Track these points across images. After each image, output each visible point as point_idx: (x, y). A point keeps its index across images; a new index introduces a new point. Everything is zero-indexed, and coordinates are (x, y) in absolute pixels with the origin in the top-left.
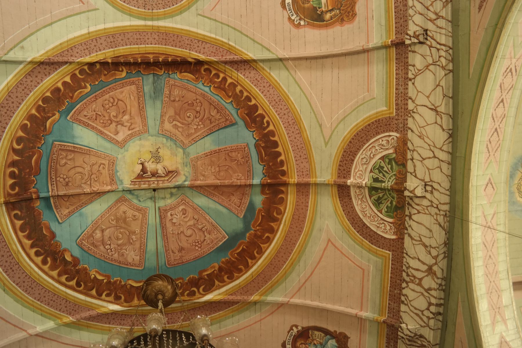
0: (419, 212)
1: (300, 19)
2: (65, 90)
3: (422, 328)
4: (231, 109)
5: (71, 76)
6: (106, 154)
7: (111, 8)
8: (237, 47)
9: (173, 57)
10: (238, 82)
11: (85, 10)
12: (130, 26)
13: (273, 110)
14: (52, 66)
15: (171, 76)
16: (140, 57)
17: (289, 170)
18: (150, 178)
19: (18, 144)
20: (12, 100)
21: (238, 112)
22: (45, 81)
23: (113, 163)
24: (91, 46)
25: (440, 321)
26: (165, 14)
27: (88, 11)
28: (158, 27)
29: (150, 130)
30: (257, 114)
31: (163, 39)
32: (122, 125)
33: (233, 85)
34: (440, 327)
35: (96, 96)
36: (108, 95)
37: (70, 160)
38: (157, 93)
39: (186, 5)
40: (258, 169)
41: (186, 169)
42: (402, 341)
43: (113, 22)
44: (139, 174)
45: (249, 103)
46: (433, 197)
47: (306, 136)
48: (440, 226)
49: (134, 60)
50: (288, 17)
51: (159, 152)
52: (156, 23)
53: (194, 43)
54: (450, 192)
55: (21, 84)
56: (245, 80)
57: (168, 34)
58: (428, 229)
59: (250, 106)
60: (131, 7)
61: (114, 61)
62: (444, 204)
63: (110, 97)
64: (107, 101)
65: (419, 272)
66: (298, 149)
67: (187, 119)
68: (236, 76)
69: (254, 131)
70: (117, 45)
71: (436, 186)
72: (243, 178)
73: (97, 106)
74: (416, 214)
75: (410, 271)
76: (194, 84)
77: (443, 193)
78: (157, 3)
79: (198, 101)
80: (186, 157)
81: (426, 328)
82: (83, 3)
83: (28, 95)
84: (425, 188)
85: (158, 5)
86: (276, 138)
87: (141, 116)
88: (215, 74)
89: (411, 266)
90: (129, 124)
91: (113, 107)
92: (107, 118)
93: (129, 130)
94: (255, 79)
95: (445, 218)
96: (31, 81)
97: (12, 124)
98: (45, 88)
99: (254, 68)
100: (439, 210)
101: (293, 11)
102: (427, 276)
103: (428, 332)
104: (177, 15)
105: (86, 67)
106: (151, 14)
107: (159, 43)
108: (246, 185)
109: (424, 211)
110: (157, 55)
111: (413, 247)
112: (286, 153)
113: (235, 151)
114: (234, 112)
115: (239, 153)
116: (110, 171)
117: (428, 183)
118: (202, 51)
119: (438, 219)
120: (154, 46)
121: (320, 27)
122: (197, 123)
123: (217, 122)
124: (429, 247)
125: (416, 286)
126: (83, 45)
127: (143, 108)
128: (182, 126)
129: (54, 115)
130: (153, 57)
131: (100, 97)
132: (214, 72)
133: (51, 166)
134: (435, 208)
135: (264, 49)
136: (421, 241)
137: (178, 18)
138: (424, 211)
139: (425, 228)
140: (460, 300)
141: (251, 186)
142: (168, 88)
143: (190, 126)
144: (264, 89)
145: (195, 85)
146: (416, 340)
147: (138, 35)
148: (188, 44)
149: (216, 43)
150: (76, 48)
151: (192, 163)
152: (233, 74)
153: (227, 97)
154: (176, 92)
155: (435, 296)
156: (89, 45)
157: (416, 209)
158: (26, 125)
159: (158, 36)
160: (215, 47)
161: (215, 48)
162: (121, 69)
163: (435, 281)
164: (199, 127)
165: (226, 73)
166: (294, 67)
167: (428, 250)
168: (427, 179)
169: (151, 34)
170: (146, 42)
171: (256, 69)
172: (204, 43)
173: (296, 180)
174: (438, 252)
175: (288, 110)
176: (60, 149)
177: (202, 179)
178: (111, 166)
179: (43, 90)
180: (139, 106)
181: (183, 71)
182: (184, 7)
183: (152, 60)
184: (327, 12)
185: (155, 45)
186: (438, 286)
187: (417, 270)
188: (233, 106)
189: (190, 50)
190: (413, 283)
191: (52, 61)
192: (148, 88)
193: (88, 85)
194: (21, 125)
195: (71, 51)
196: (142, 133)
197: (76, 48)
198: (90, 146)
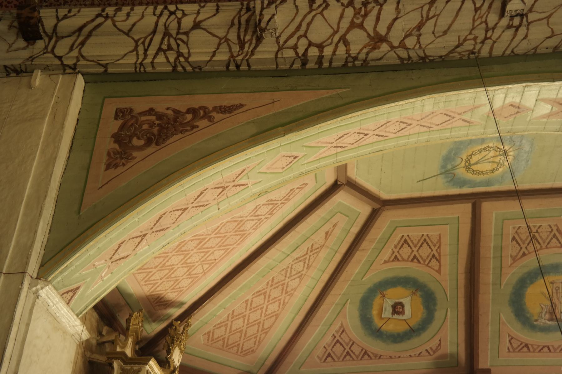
0: (476, 10)
3: (275, 39)
25: (291, 66)
34: (282, 67)
42: (242, 8)
46: (501, 30)
48: (458, 46)
54: (509, 55)
58: (449, 28)
62: (492, 48)
65: (373, 23)
71: (522, 31)
74: (475, 5)
75: (374, 7)
77: (510, 44)
81: (276, 45)
84: (517, 15)
89: (384, 7)
95: (468, 53)
100: (483, 42)
102: (369, 35)
103: (271, 49)
109: (478, 19)
111: (418, 6)
117: (525, 19)
119: (468, 42)
124: (417, 33)
125: (350, 19)
134: (486, 34)
136: (428, 19)
138: (478, 19)
139: (450, 22)
140: (339, 91)
146: (250, 32)
155: (337, 53)
157: (482, 5)
163: (361, 50)
167: (413, 33)
168: (532, 17)
174: (413, 49)
186: (353, 55)
187: (378, 19)
190: (355, 14)
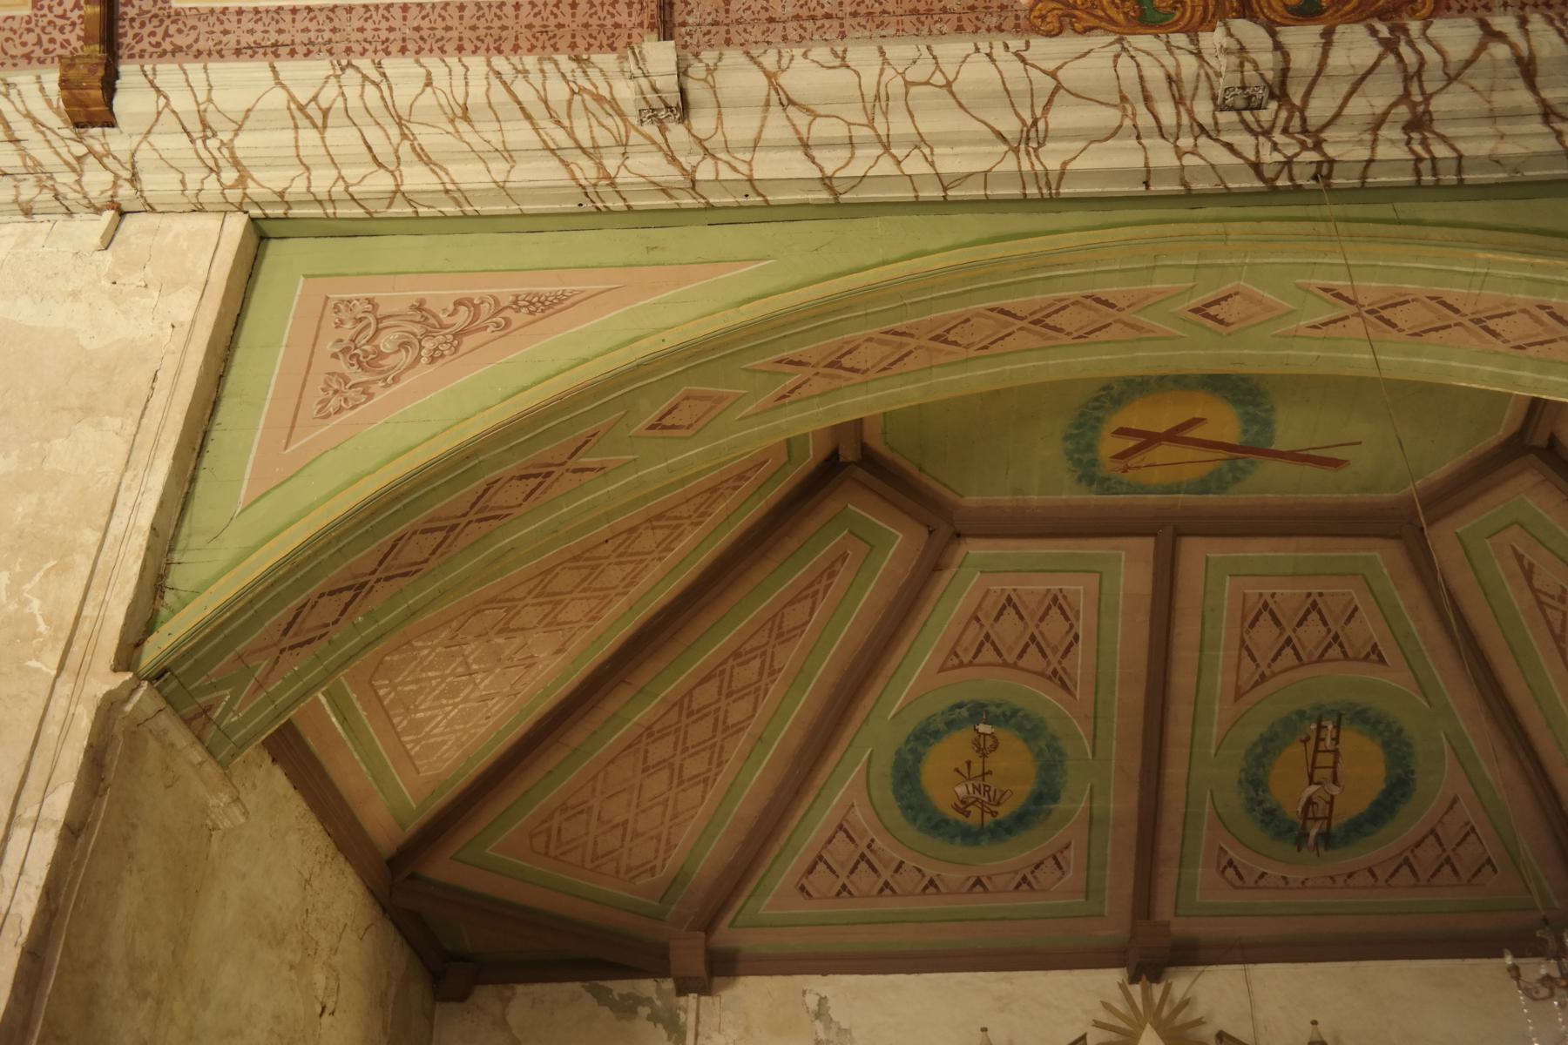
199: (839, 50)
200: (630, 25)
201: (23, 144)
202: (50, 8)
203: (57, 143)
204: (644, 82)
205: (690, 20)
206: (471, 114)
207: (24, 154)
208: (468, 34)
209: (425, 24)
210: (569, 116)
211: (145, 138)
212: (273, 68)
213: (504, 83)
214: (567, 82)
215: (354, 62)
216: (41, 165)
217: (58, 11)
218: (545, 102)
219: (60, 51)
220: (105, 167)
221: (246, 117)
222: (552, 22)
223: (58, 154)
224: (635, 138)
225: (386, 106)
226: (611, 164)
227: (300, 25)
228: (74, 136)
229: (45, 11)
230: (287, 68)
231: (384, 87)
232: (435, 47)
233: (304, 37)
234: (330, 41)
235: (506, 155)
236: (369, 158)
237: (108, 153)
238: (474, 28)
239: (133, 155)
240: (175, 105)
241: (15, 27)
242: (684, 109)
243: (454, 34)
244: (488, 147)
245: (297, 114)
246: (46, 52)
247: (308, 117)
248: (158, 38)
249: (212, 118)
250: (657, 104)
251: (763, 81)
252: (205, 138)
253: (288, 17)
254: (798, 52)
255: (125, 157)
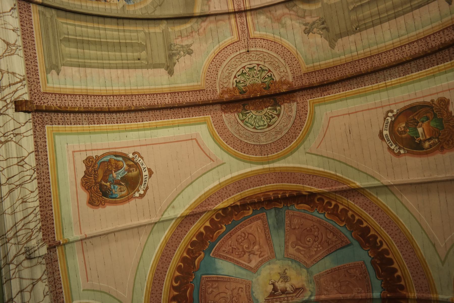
1: (400, 148)
2: (206, 233)
4: (345, 232)
5: (210, 221)
6: (243, 279)
7: (235, 160)
8: (344, 177)
9: (290, 191)
10: (349, 208)
11: (215, 166)
12: (251, 171)
13: (384, 231)
14: (195, 216)
15: (290, 208)
16: (263, 196)
17: (407, 285)
18: (281, 295)
19: (176, 282)
20: (170, 249)
21: (351, 234)
22: (192, 228)
23: (249, 286)
24: (223, 193)
26: (278, 157)
27: (217, 166)
28: (274, 168)
29: (277, 255)
30: (369, 235)
31: (279, 178)
32: (254, 254)
33: (345, 211)
35: (230, 234)
36: (240, 231)
37: (215, 288)
38: (279, 224)
39: (295, 146)
40: (377, 283)
41: (311, 285)
43: (238, 171)
44: (271, 292)
45: (361, 226)
47: (420, 254)
49: (257, 200)
50: (387, 147)
51: (286, 273)
52: (272, 166)
53: (306, 177)
55: (174, 235)
56: (355, 206)
57: (283, 173)
59: (362, 228)
60: (250, 156)
61: (242, 204)
63: (242, 232)
64: (240, 237)
66: (414, 266)
67: (307, 243)
68: (346, 202)
69: (369, 250)
70: (243, 189)
72: (363, 291)
73: (232, 242)
76: (310, 213)
78: (271, 148)
79: (315, 227)
80: (310, 276)
82: (213, 161)
83: (180, 242)
85: (272, 150)
86: (391, 256)
87: (268, 245)
88: (327, 203)
90: (259, 253)
91: (245, 240)
92: (241, 250)
93: (260, 257)
94: (364, 204)
96: (182, 231)
97: (171, 267)
98: (192, 235)
99: (361, 194)
101: (391, 142)
104: (288, 156)
105: (220, 212)
106: (267, 158)
107: (276, 182)
108: (366, 299)
110: (276, 192)
112: (402, 269)
113: (353, 269)
114: (348, 234)
115: (356, 270)
116: (248, 293)
118: (313, 184)
120: (273, 184)
121: (420, 155)
122: (316, 246)
123: (334, 244)
126: (217, 194)
127: (270, 238)
128: (304, 249)
129: (200, 254)
130: (273, 194)
131: (234, 234)
132: (326, 201)
133: (201, 295)
135: (369, 177)
137: (290, 158)
141: (372, 299)
142: (289, 218)
143: (311, 249)
144: (374, 212)
145: (311, 213)
147: (258, 177)
148: (301, 179)
149: (325, 175)
150: (211, 197)
151: (315, 280)
152: (343, 201)
153: (341, 222)
154: (296, 221)
156: (221, 193)
158: (180, 266)
159: (275, 175)
160: (325, 179)
161: (324, 180)
162: (248, 208)
164: (319, 249)
165: (337, 201)
166: (400, 192)
169: (269, 175)
170: (266, 183)
171: (364, 195)
172: (315, 177)
173: (416, 296)
175: (399, 231)
176: (207, 281)
177: (325, 293)
178: (248, 289)
179: (190, 236)
180: (266, 237)
181: (299, 202)
182: (293, 148)
183: (272, 197)
184: (425, 141)
185: (273, 183)
188: (347, 229)
189: (303, 184)
191: (195, 213)
192: (271, 221)
193: (223, 226)
194: (178, 266)
195: (208, 201)
196: (271, 258)
197: (211, 197)
198: (230, 275)
199: (48, 293)
200: (49, 238)
201: (9, 87)
202: (43, 96)
203: (10, 96)
204: (37, 248)
205: (52, 253)
206: (24, 204)
207: (6, 87)
208: (44, 199)
209: (46, 188)
210: (25, 229)
211: (12, 118)
212: (33, 152)
213: (33, 211)
214: (35, 227)
215: (36, 172)
216: (3, 91)
217: (43, 98)
218: (29, 222)
219: (33, 98)
220: (3, 107)
221: (20, 145)
222: (48, 219)
223: (7, 95)
224: (20, 246)
225: (25, 182)
226: (12, 241)
227: (43, 157)
228: (12, 100)
229: (42, 95)
230: (33, 156)
231: (30, 181)
232: (40, 191)
233: (40, 158)
234: (40, 164)
235: (13, 213)
236: (10, 176)
237: (8, 109)
238: (45, 200)
239: (7, 115)
240: (22, 128)
241: (38, 88)
242: (29, 258)
243: (44, 195)
244: (15, 208)
245: (21, 159)
246: (33, 95)
247: (21, 161)
248: (38, 122)
249: (19, 137)
250: (31, 252)
251: (39, 277)
252: (13, 134)
253: (45, 154)
254: (47, 283)
255: (7, 112)
